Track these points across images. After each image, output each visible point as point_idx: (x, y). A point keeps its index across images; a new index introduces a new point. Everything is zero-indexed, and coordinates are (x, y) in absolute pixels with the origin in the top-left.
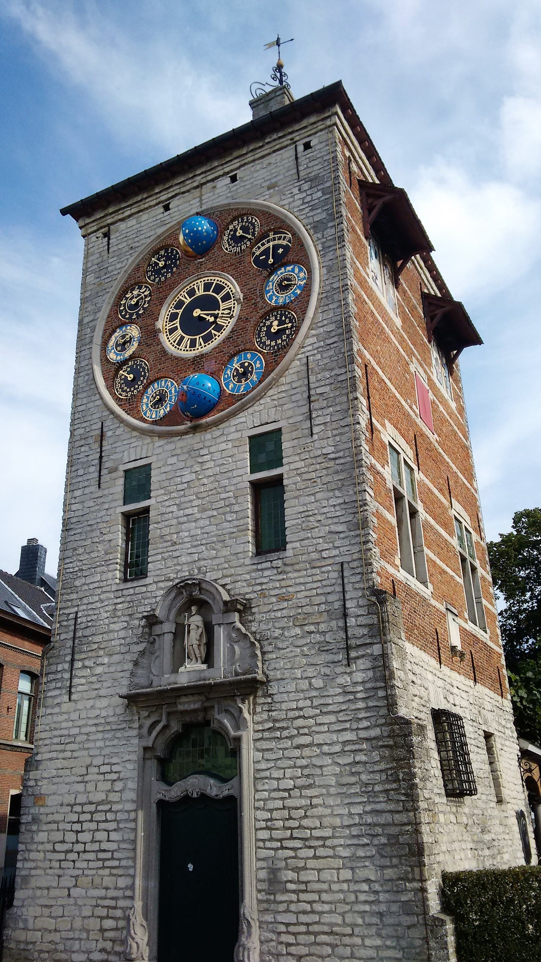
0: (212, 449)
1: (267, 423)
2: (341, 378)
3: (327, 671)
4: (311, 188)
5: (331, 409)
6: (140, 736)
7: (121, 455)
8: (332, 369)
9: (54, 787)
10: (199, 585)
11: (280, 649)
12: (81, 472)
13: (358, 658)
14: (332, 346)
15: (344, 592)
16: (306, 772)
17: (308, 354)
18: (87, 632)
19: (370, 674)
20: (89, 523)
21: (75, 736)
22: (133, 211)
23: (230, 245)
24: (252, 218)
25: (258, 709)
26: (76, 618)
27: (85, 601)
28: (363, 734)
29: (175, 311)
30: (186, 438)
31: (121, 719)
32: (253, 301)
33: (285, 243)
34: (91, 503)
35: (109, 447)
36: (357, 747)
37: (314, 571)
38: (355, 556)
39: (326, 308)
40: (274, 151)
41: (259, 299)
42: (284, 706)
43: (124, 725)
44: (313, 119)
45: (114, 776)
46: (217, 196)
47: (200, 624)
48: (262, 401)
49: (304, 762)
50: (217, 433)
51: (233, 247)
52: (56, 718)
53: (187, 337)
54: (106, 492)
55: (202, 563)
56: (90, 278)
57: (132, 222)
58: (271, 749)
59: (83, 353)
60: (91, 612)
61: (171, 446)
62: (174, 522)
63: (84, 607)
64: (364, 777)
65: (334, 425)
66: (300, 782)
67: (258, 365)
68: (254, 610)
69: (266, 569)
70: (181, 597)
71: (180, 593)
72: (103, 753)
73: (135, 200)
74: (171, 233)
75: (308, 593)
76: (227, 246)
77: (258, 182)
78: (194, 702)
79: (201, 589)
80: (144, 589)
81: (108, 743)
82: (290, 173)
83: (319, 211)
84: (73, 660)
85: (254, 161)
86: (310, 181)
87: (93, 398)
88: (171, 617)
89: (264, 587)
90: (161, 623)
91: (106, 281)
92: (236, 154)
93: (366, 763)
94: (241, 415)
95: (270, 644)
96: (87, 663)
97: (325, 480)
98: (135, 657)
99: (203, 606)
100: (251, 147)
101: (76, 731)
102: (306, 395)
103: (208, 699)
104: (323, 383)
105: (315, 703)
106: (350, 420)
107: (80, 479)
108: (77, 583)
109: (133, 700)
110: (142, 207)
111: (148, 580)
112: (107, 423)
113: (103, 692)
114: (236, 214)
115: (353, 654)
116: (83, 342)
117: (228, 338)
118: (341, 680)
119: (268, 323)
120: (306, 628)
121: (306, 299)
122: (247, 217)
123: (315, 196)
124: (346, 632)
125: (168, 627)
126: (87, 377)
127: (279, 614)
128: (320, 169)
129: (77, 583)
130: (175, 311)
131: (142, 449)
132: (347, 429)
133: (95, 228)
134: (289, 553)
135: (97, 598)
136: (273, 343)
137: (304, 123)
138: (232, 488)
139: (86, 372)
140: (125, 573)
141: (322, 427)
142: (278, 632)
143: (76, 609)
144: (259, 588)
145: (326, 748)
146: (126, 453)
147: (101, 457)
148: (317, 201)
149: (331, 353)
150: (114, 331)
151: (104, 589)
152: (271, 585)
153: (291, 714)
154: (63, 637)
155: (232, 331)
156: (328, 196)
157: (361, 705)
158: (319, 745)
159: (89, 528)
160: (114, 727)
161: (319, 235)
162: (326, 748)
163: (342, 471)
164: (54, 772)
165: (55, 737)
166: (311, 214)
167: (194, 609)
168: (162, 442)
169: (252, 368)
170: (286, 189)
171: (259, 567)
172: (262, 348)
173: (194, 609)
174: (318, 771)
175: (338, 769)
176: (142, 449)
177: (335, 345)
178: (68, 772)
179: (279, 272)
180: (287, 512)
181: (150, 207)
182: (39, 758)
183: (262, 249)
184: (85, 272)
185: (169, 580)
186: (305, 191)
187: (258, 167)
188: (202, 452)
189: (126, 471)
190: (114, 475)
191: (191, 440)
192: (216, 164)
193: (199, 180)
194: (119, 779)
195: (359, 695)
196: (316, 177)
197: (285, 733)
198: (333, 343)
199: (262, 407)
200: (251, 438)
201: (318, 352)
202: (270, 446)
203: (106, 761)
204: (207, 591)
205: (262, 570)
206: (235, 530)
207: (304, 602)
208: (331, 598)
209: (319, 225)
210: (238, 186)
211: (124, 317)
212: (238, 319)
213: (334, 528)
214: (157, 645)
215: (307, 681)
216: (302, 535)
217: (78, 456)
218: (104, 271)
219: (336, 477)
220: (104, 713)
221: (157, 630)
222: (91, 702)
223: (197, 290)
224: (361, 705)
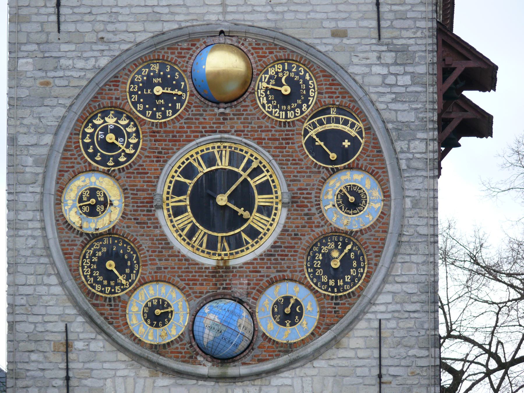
4: (396, 64)
7: (101, 383)
8: (411, 347)
14: (412, 315)
17: (379, 316)
23: (269, 102)
24: (306, 72)
29: (182, 179)
30: (205, 386)
32: (306, 210)
33: (353, 133)
35: (80, 366)
39: (407, 258)
41: (314, 210)
46: (249, 9)
48: (316, 363)
51: (275, 107)
56: (25, 65)
59: (22, 197)
74: (173, 44)
76: (265, 102)
77: (318, 16)
82: (365, 23)
83: (406, 106)
86: (396, 52)
87: (46, 280)
91: (57, 82)
94: (286, 374)
102: (376, 372)
114: (281, 54)
116: (20, 177)
117: (268, 254)
119: (324, 249)
121: (383, 235)
122: (298, 67)
126: (31, 242)
128: (410, 38)
130: (182, 179)
131: (135, 383)
136: (332, 283)
139: (29, 232)
146: (109, 382)
147: (68, 378)
148: (403, 90)
155: (274, 246)
156: (419, 89)
166: (393, 106)
169: (301, 309)
170: (360, 48)
172: (316, 284)
176: (135, 383)
177: (416, 315)
179: (343, 178)
183: (320, 129)
184: (14, 48)
186: (388, 65)
196: (402, 50)
198: (414, 312)
199: (314, 372)
201: (394, 318)
209: (405, 129)
210: (286, 9)
211: (92, 156)
212: (283, 230)
217: (27, 367)
218: (51, 64)
223: (217, 157)
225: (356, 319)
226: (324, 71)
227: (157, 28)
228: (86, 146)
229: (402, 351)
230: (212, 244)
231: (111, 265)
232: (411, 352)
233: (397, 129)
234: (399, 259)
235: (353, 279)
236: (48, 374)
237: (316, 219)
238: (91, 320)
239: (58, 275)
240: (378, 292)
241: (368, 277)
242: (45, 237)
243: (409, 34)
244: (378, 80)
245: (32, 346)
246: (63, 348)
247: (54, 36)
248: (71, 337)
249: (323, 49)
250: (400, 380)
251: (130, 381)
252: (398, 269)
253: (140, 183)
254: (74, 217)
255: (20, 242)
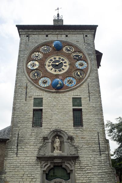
0: (62, 98)
1: (77, 96)
2: (97, 90)
3: (95, 156)
5: (94, 96)
6: (41, 168)
8: (95, 87)
9: (11, 179)
10: (60, 131)
11: (82, 150)
12: (19, 95)
13: (102, 154)
15: (99, 139)
16: (89, 179)
18: (22, 139)
19: (105, 158)
20: (22, 109)
21: (19, 166)
22: (37, 33)
25: (76, 164)
26: (18, 135)
27: (21, 130)
28: (103, 171)
31: (34, 163)
33: (81, 55)
34: (23, 104)
36: (102, 174)
37: (91, 133)
38: (101, 131)
40: (78, 34)
42: (83, 163)
43: (35, 164)
44: (89, 31)
45: (33, 177)
47: (59, 141)
48: (76, 90)
49: (90, 176)
50: (64, 95)
52: (11, 161)
53: (53, 69)
54: (27, 102)
55: (60, 126)
57: (36, 36)
58: (80, 173)
59: (20, 64)
60: (23, 134)
61: (49, 95)
62: (51, 114)
63: (21, 132)
64: (104, 180)
65: (95, 100)
66: (87, 181)
67: (74, 81)
68: (75, 140)
69: (78, 130)
70: (54, 134)
71: (54, 133)
72: (29, 171)
73: (38, 31)
75: (89, 138)
78: (59, 160)
79: (60, 132)
80: (41, 130)
81: (30, 169)
84: (17, 146)
85: (72, 34)
88: (51, 138)
89: (77, 134)
90: (48, 139)
92: (68, 31)
93: (104, 177)
95: (80, 148)
96: (23, 147)
97: (93, 112)
98: (39, 147)
99: (60, 137)
100: (72, 31)
101: (19, 165)
102: (88, 91)
103: (63, 160)
104: (92, 90)
105: (92, 163)
106: (99, 100)
107: (18, 97)
108: (19, 125)
109: (39, 158)
110: (40, 33)
111: (42, 128)
112: (28, 84)
113: (27, 155)
115: (101, 153)
116: (20, 61)
117: (65, 73)
118: (98, 159)
119: (77, 72)
120: (89, 146)
123: (89, 48)
124: (100, 148)
125: (50, 141)
126: (21, 71)
127: (81, 142)
129: (19, 125)
132: (98, 102)
133: (25, 33)
134: (84, 128)
135: (25, 130)
137: (86, 31)
138: (68, 109)
140: (33, 125)
141: (92, 100)
142: (81, 146)
143: (18, 132)
144: (76, 135)
145: (95, 174)
146: (35, 94)
147: (26, 93)
149: (94, 83)
150: (30, 61)
151: (28, 128)
152: (79, 134)
153: (85, 165)
154: (13, 139)
155: (67, 71)
157: (103, 164)
158: (93, 173)
159: (22, 111)
160: (32, 165)
161: (90, 56)
162: (95, 174)
163: (97, 111)
164: (11, 175)
165: (11, 166)
167: (57, 137)
168: (46, 93)
171: (76, 129)
173: (57, 137)
174: (93, 179)
175: (97, 178)
178: (17, 175)
180: (83, 118)
181: (42, 34)
182: (6, 171)
183: (75, 54)
184: (21, 44)
185: (49, 129)
187: (74, 36)
188: (59, 98)
189: (34, 98)
190: (30, 98)
191: (55, 95)
192: (63, 31)
193: (57, 33)
194: (34, 178)
195: (103, 162)
196: (89, 44)
197: (84, 170)
200: (73, 98)
202: (78, 101)
203: (30, 173)
204: (61, 133)
205: (77, 130)
206: (69, 119)
207: (89, 140)
208: (95, 140)
213: (95, 124)
214: (46, 145)
215: (89, 158)
216: (88, 124)
218: (27, 45)
219: (96, 112)
220: (28, 161)
221: (46, 141)
222: (24, 158)
224: (103, 164)
225: (84, 82)
226: (75, 46)
227: (46, 41)
228: (32, 57)
229: (93, 88)
230: (55, 71)
231: (36, 74)
232: (95, 88)
233: (89, 54)
234: (91, 73)
235: (82, 77)
236: (22, 92)
237: (75, 67)
238: (32, 83)
239: (26, 76)
240: (87, 78)
241: (85, 76)
242: (24, 70)
243: (89, 42)
244: (85, 48)
245: (20, 87)
246: (26, 88)
247: (28, 42)
248: (27, 86)
249: (75, 44)
250: (93, 93)
251: (39, 93)
252: (91, 75)
253: (42, 62)
254: (30, 67)
255: (19, 71)
